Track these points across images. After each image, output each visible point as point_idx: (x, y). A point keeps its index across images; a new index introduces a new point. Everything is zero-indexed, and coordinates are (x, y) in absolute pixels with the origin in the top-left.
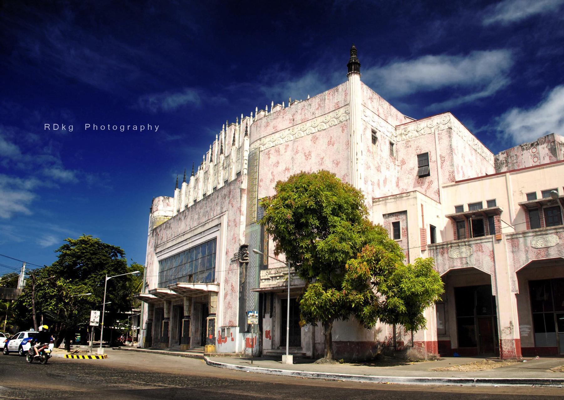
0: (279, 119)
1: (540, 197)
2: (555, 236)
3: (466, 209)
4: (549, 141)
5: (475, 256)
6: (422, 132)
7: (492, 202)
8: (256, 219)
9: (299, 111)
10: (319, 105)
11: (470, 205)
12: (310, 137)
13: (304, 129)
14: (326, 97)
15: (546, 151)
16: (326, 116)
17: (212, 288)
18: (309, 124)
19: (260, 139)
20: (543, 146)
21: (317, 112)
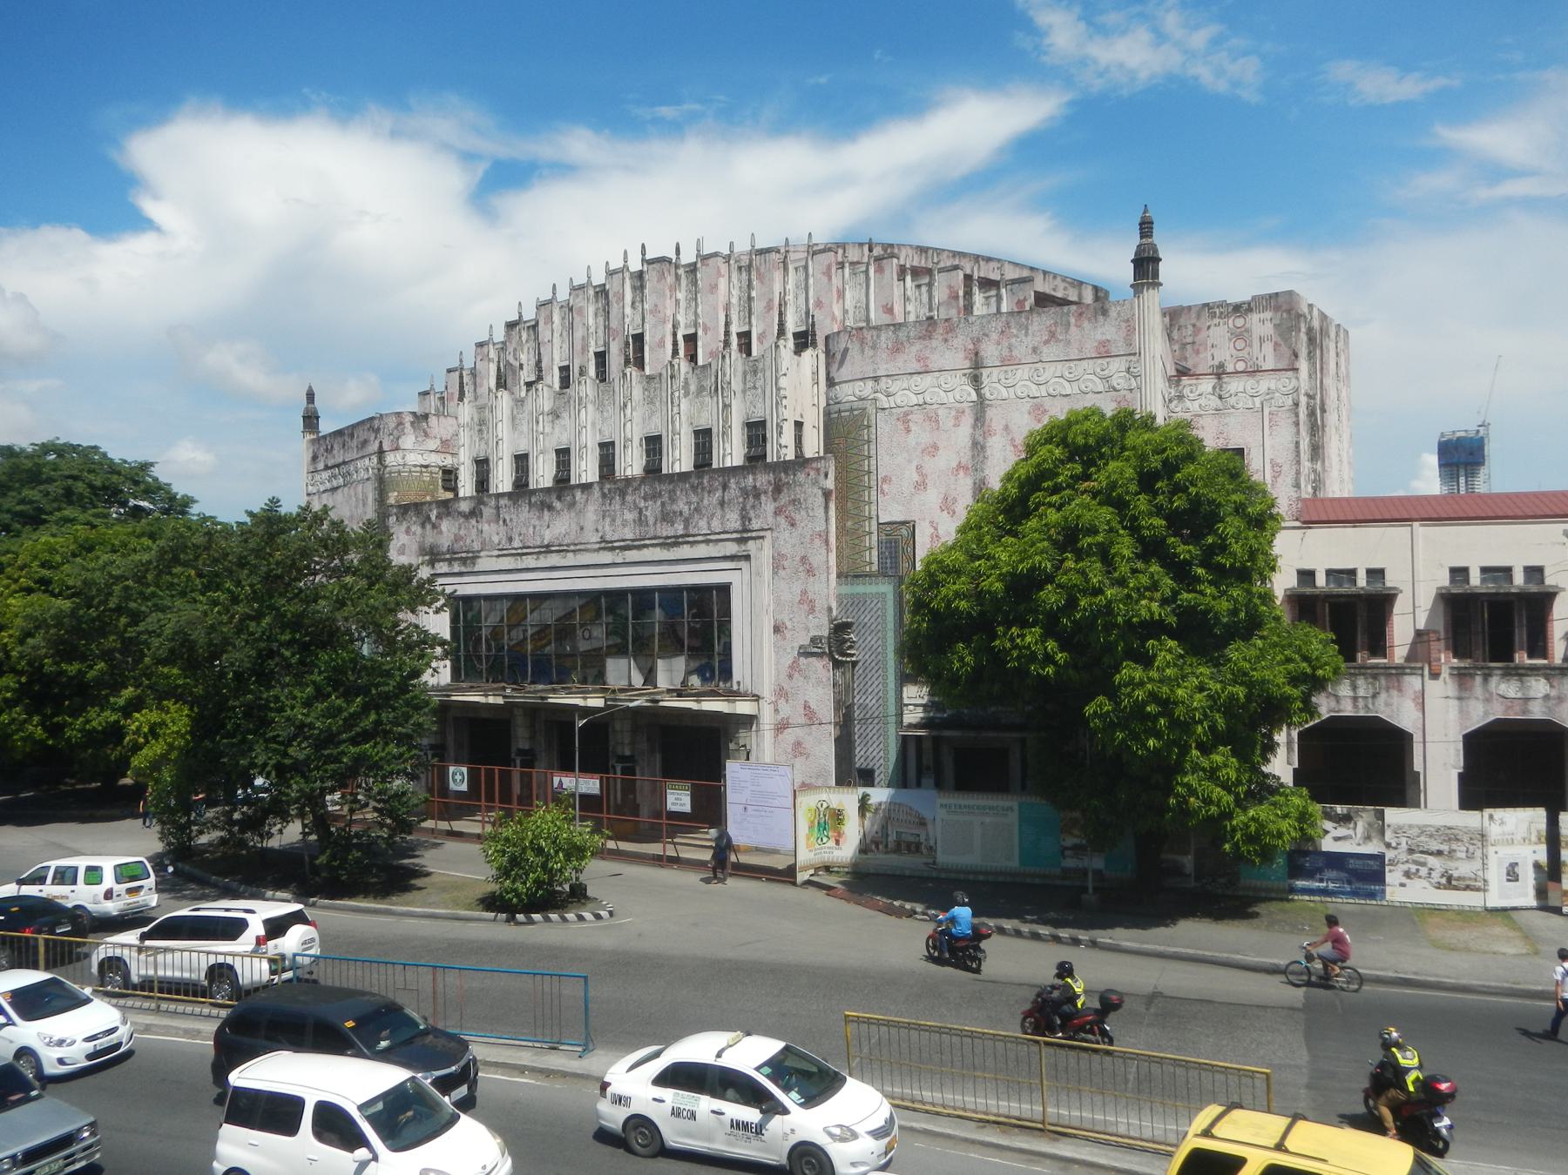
0: (934, 343)
1: (1475, 579)
2: (1543, 681)
3: (1321, 580)
4: (1277, 309)
5: (1383, 696)
6: (1232, 401)
7: (1376, 574)
8: (875, 568)
9: (994, 336)
10: (1052, 335)
11: (1329, 573)
12: (1027, 405)
13: (1010, 382)
14: (1073, 320)
15: (1268, 329)
16: (1072, 364)
17: (743, 708)
18: (1023, 373)
19: (876, 379)
20: (1262, 316)
21: (1045, 350)
